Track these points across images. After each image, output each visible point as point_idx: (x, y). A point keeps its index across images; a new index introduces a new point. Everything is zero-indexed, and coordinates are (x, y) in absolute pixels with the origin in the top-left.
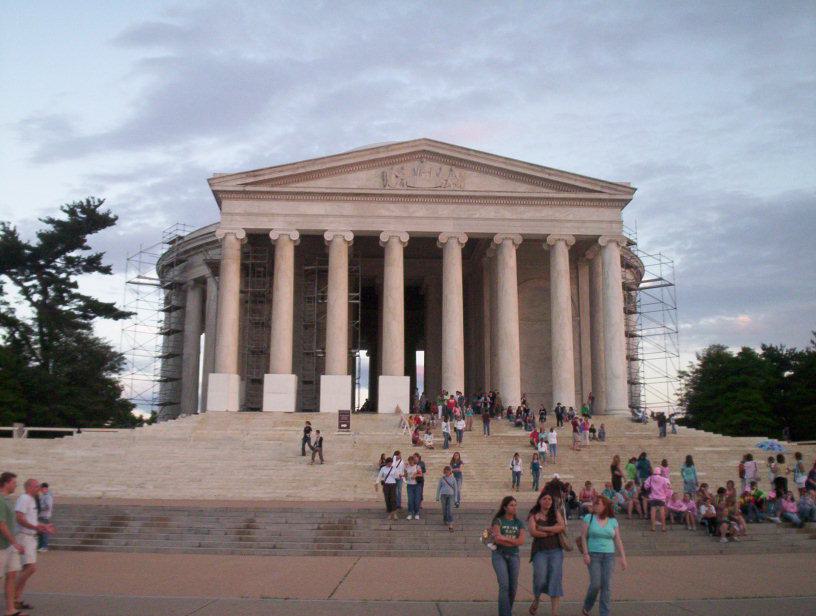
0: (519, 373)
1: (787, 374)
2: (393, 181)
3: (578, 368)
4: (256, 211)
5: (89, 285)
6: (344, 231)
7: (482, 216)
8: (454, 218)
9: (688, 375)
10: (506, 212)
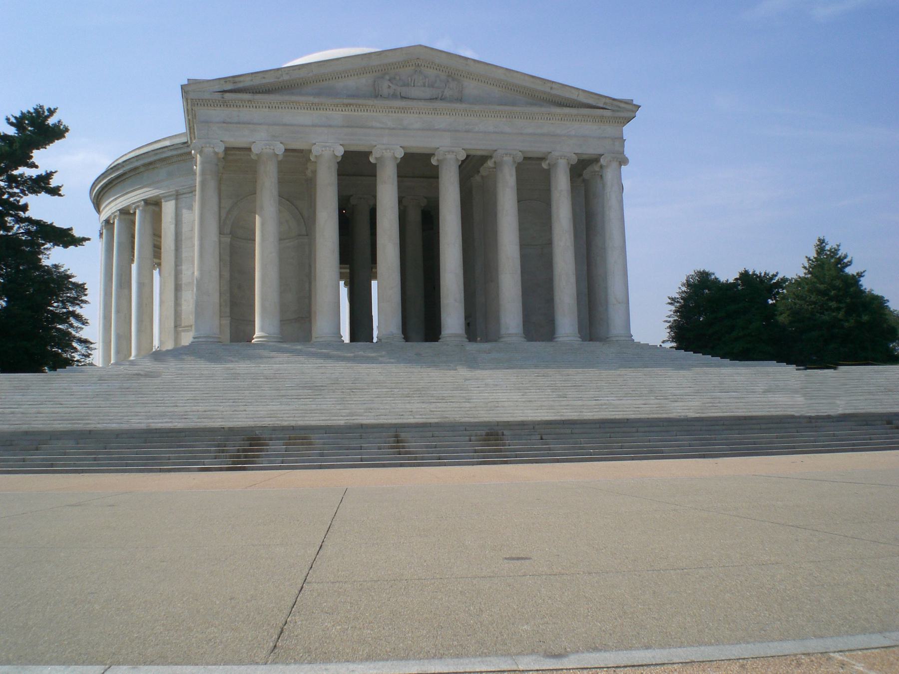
1: (770, 302)
5: (39, 207)
9: (678, 302)
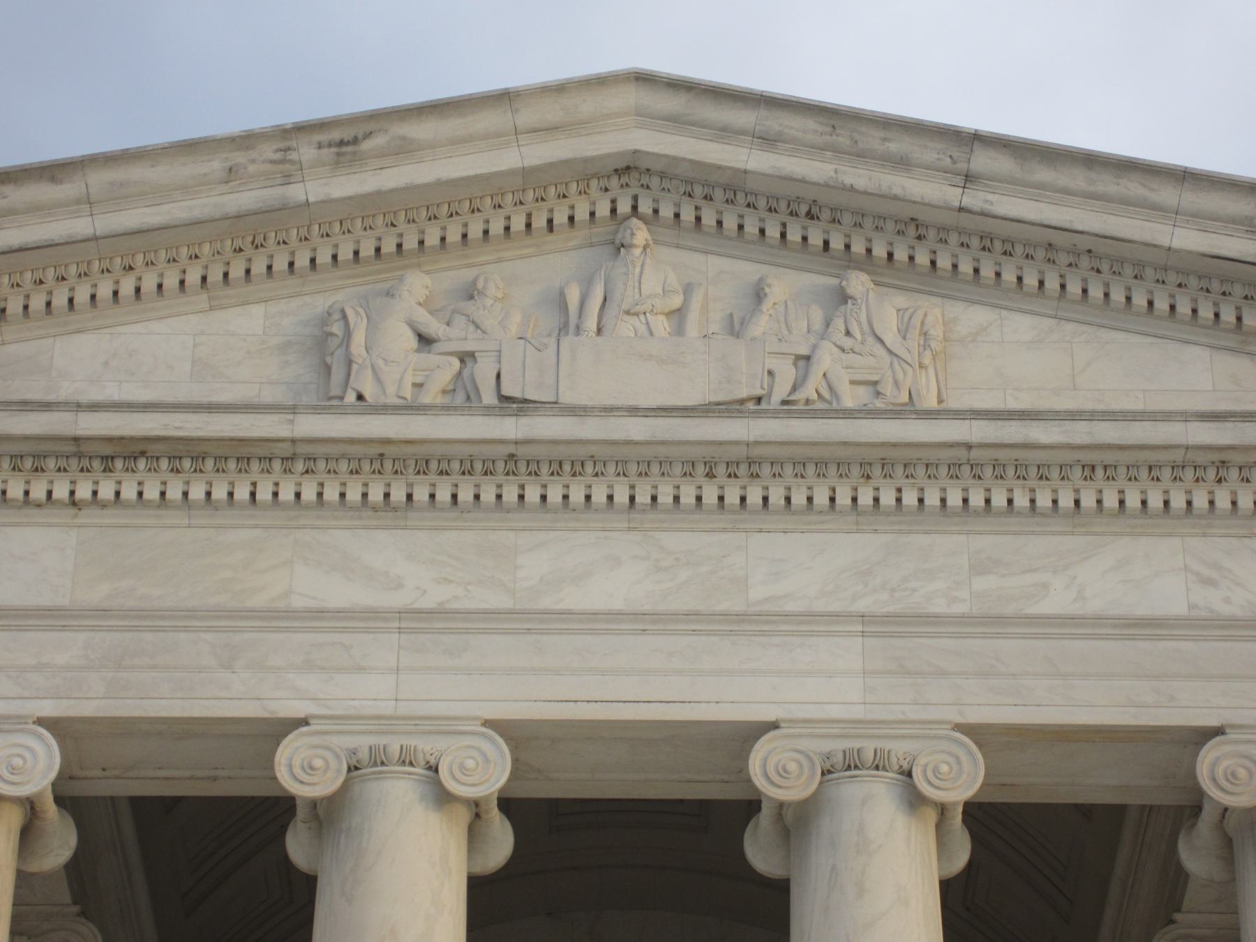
2: (390, 356)
7: (1094, 606)
8: (873, 624)
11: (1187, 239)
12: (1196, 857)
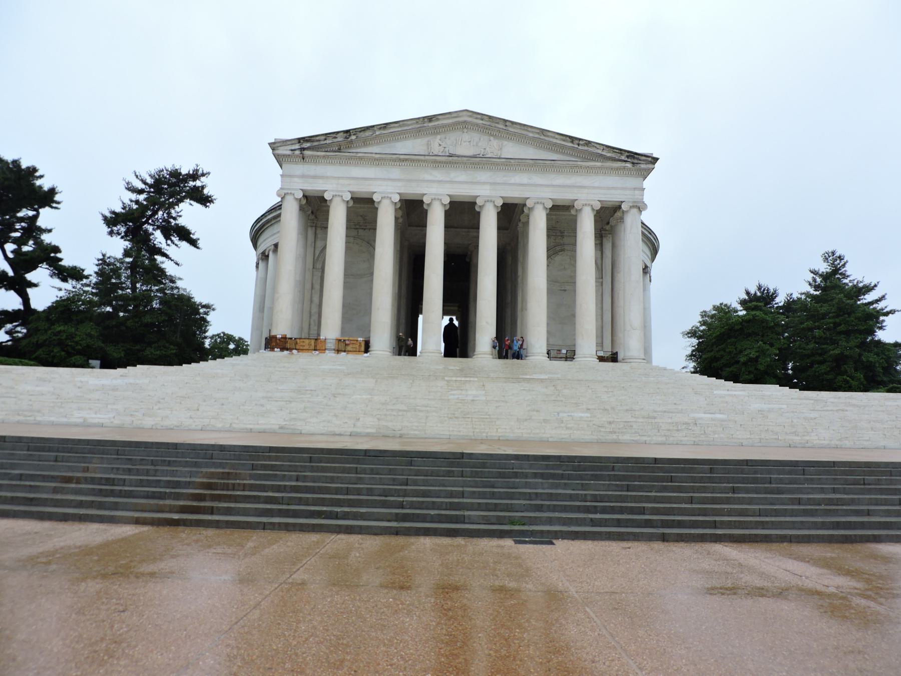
0: (545, 325)
3: (600, 323)
4: (312, 173)
6: (392, 193)
8: (491, 184)
10: (537, 179)
11: (531, 135)
12: (526, 210)
